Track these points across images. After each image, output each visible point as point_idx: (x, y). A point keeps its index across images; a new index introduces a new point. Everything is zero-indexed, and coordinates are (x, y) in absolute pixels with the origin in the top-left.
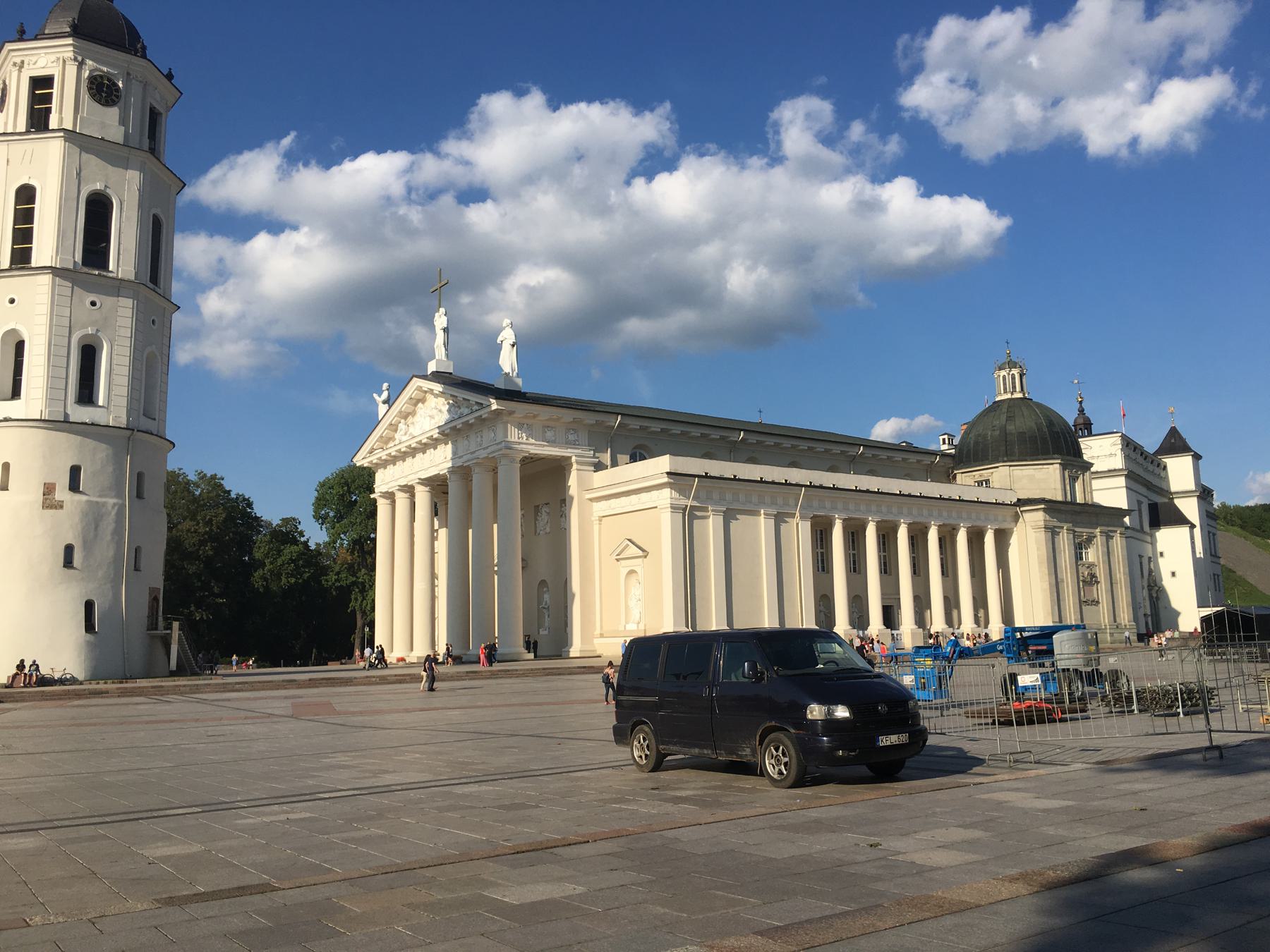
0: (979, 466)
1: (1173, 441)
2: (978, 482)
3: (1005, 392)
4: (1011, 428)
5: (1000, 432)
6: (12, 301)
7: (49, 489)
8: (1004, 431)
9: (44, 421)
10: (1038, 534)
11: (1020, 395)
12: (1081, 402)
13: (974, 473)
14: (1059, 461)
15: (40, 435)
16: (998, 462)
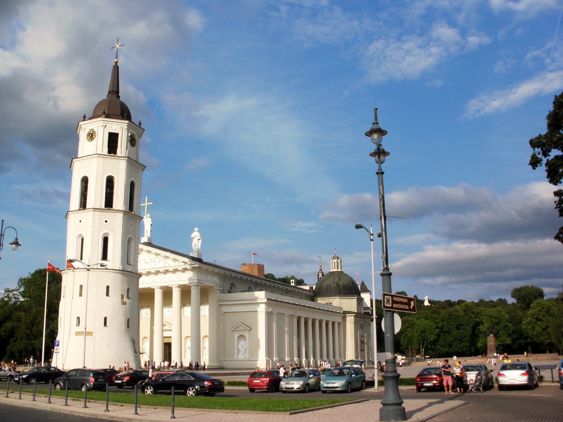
0: (327, 297)
1: (363, 287)
2: (327, 303)
3: (335, 268)
4: (340, 283)
5: (337, 284)
6: (106, 221)
7: (122, 298)
8: (337, 283)
9: (120, 270)
10: (351, 325)
11: (340, 270)
12: (321, 266)
13: (326, 300)
14: (357, 298)
15: (119, 277)
16: (337, 296)
